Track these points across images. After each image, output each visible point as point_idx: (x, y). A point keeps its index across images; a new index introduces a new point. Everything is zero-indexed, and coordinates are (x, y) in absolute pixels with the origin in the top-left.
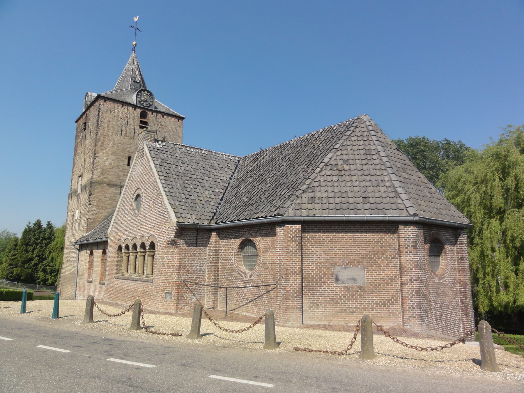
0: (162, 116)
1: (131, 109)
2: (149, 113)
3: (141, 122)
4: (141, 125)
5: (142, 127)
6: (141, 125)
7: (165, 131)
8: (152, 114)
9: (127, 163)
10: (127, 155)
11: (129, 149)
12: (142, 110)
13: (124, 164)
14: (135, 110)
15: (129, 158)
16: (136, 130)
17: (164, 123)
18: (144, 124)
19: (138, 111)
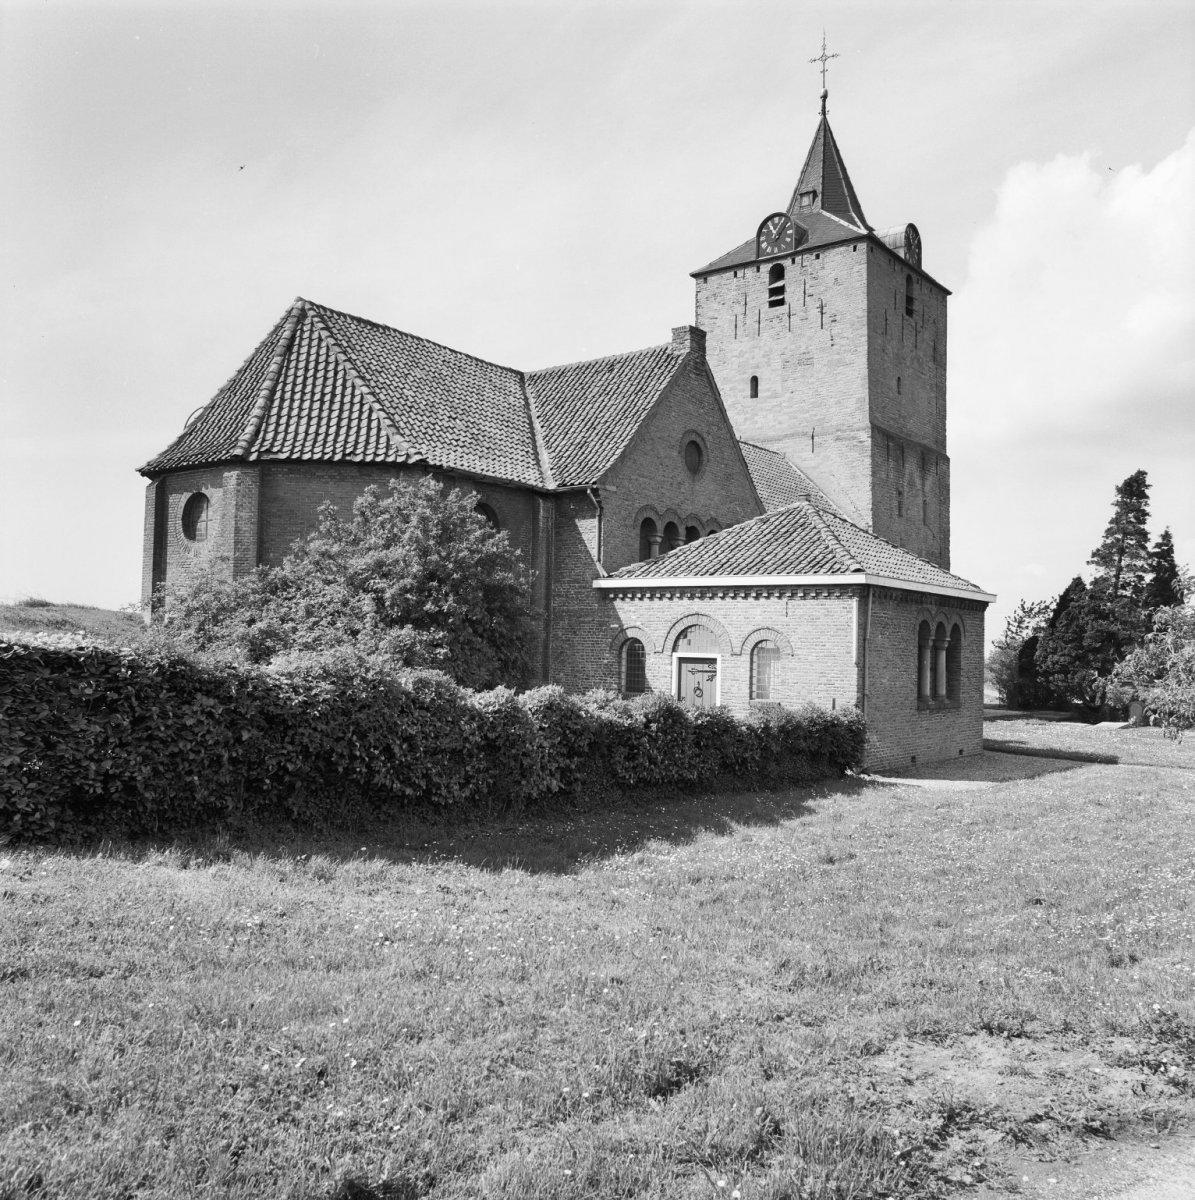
0: (813, 257)
1: (750, 272)
2: (787, 263)
3: (773, 292)
5: (773, 304)
8: (793, 261)
9: (748, 392)
11: (751, 362)
12: (771, 265)
14: (758, 271)
15: (755, 380)
17: (821, 273)
18: (777, 297)
19: (766, 268)
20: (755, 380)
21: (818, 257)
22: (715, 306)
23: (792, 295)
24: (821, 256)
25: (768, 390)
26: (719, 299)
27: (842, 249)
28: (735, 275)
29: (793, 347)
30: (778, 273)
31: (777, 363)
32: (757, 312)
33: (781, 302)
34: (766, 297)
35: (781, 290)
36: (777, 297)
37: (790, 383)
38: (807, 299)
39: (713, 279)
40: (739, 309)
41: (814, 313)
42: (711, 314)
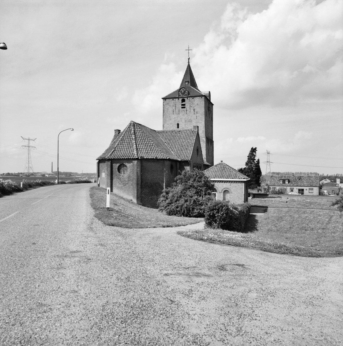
0: (192, 98)
1: (177, 100)
2: (186, 99)
3: (182, 105)
4: (182, 106)
5: (182, 108)
6: (182, 106)
7: (194, 106)
8: (187, 99)
10: (177, 123)
12: (182, 99)
13: (175, 128)
14: (179, 99)
15: (178, 125)
16: (180, 110)
18: (183, 106)
19: (180, 99)
20: (178, 125)
21: (193, 98)
22: (168, 106)
23: (187, 106)
24: (194, 98)
25: (181, 127)
26: (169, 105)
27: (199, 97)
28: (173, 100)
29: (187, 118)
30: (183, 101)
31: (183, 121)
32: (178, 109)
33: (184, 107)
34: (181, 106)
35: (184, 105)
36: (183, 106)
37: (187, 126)
38: (191, 107)
39: (167, 100)
40: (174, 108)
41: (192, 111)
42: (167, 108)
